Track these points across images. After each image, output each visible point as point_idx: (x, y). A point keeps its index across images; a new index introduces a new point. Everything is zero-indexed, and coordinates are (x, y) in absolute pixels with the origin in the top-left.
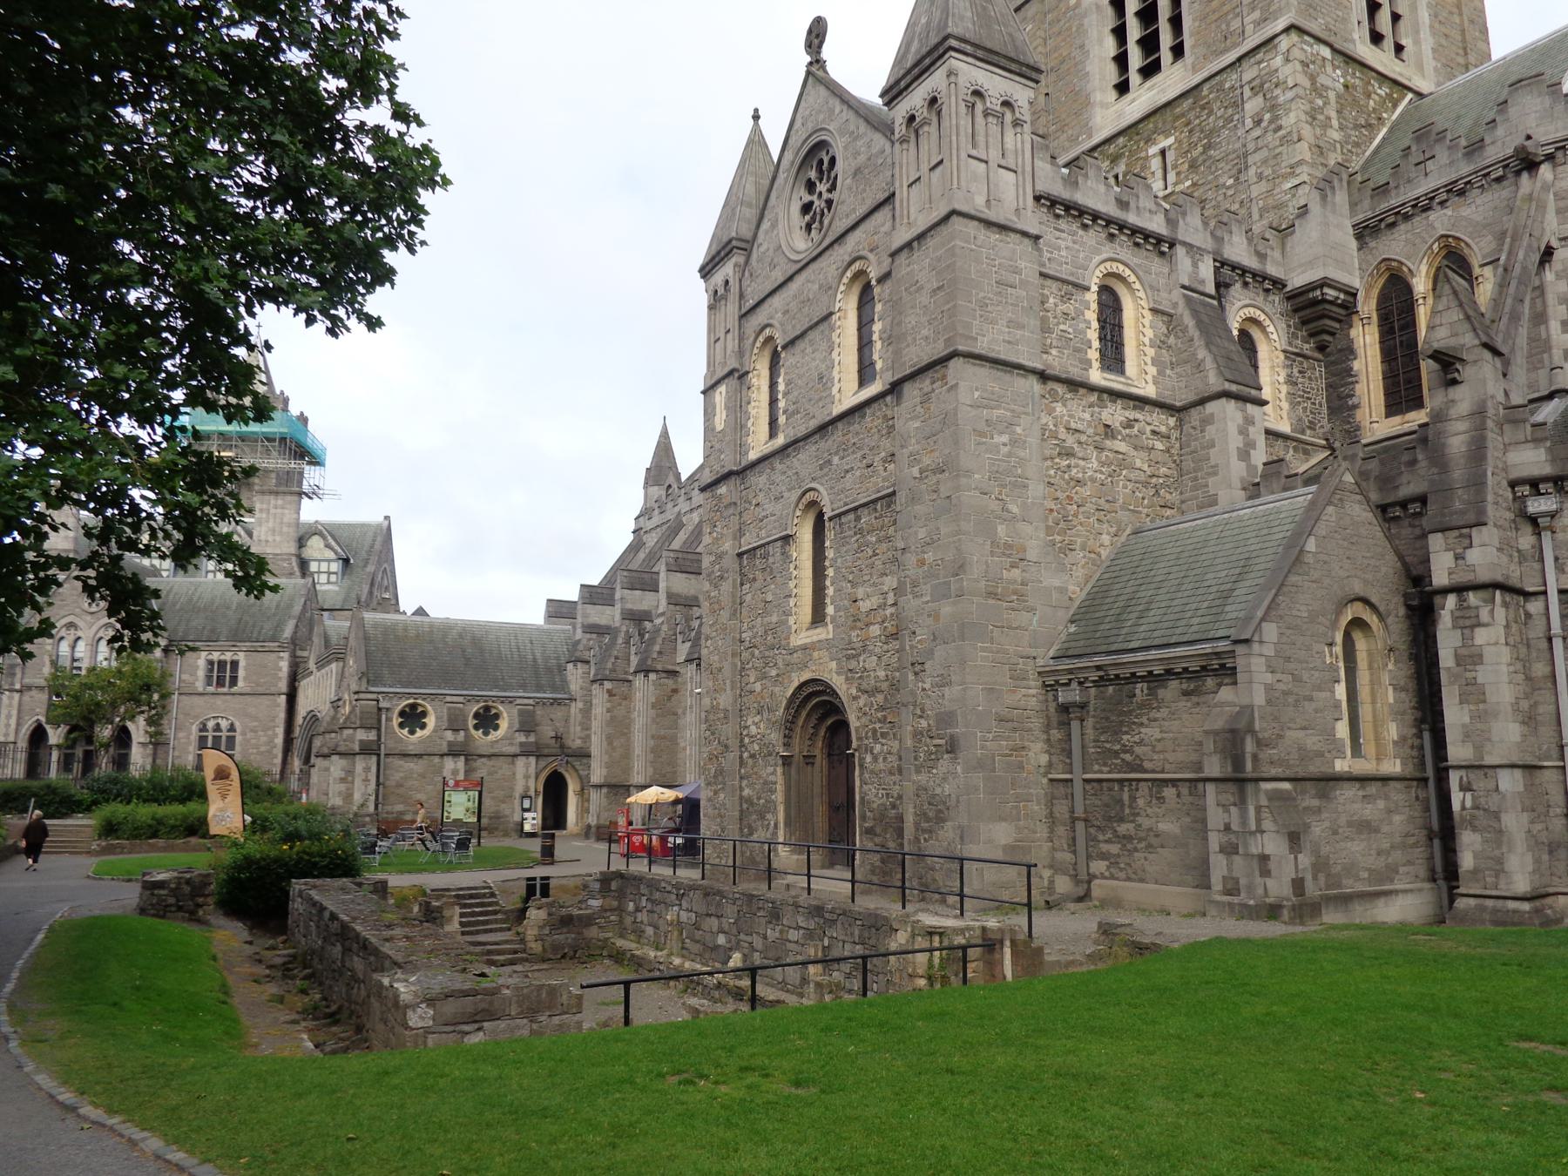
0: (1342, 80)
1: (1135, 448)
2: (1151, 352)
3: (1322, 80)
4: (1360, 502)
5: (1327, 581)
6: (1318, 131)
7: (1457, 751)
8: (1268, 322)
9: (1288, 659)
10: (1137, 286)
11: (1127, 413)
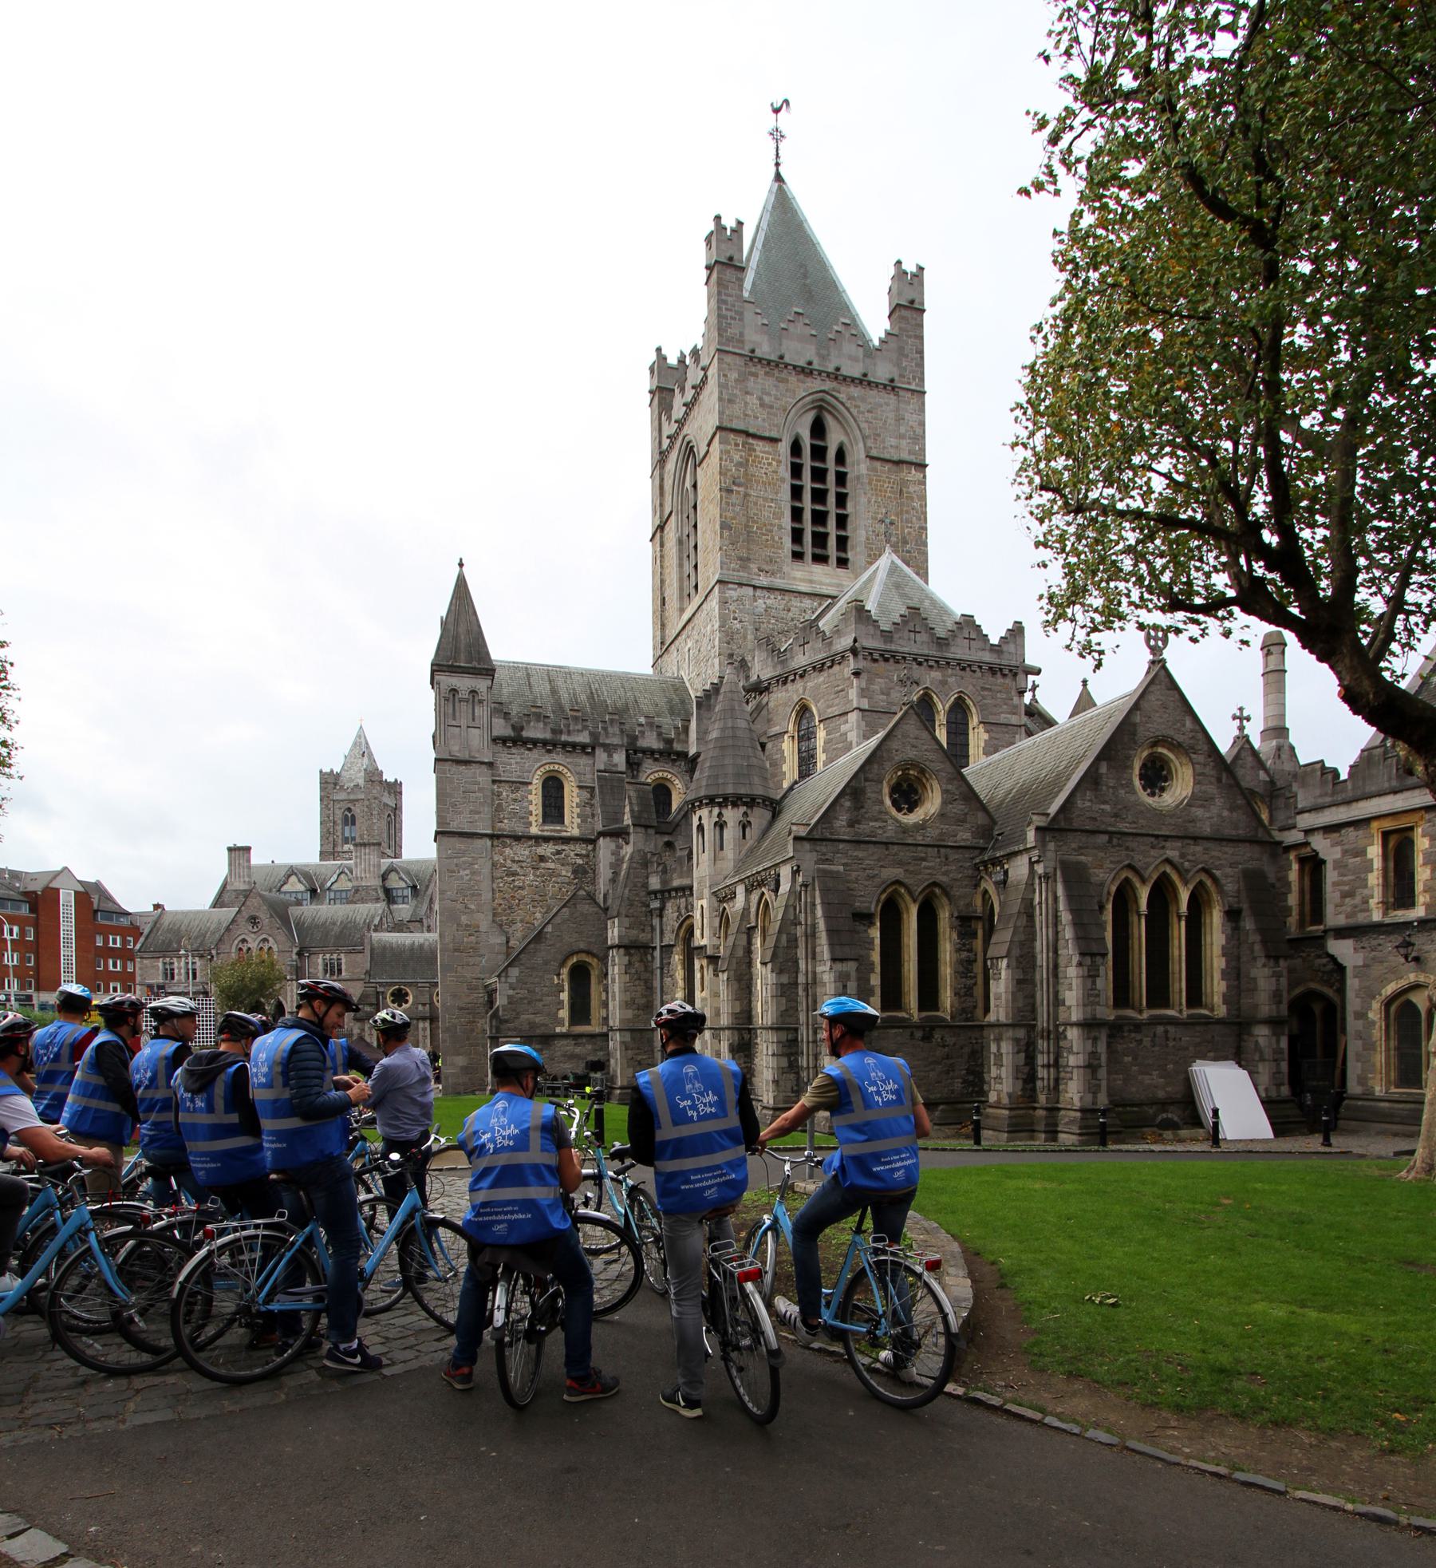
2: (578, 810)
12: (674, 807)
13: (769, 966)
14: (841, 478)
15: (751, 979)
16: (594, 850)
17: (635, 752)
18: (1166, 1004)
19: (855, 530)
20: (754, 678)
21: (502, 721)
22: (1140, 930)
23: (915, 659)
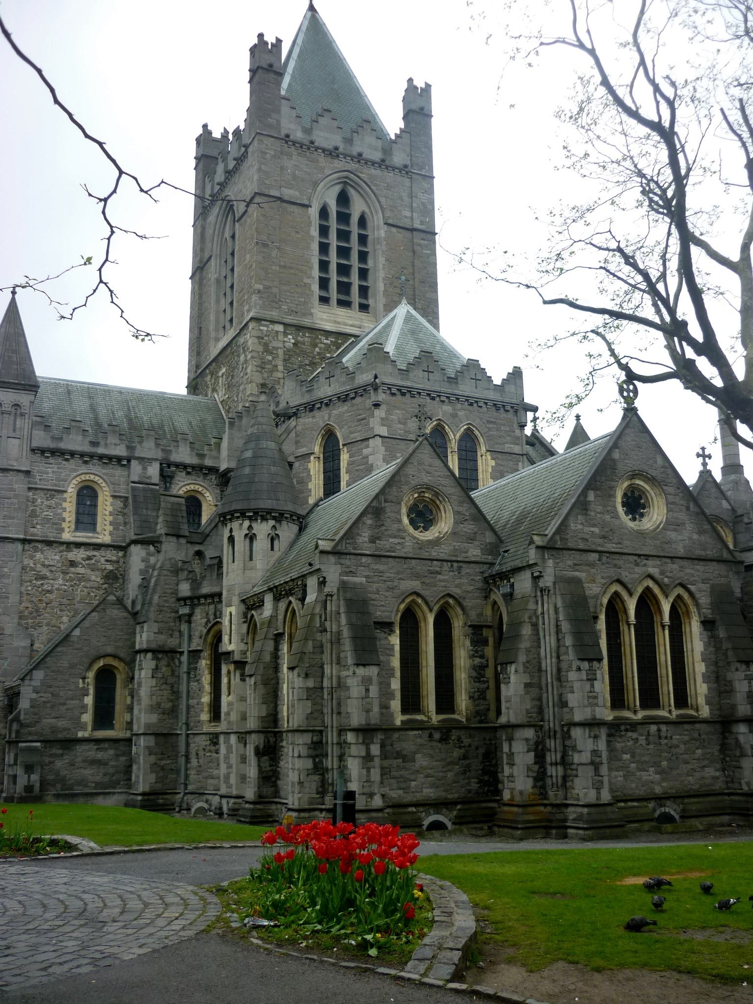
0: (293, 341)
1: (93, 570)
2: (111, 518)
3: (275, 344)
4: (118, 609)
5: (85, 649)
6: (265, 375)
7: (135, 727)
8: (205, 491)
9: (50, 687)
10: (104, 484)
11: (88, 553)
12: (204, 519)
13: (296, 671)
14: (363, 239)
15: (278, 683)
16: (124, 556)
17: (169, 466)
18: (657, 705)
19: (375, 281)
20: (283, 405)
21: (42, 433)
22: (629, 638)
23: (429, 395)
